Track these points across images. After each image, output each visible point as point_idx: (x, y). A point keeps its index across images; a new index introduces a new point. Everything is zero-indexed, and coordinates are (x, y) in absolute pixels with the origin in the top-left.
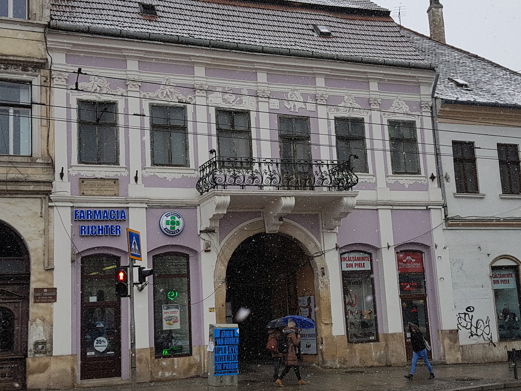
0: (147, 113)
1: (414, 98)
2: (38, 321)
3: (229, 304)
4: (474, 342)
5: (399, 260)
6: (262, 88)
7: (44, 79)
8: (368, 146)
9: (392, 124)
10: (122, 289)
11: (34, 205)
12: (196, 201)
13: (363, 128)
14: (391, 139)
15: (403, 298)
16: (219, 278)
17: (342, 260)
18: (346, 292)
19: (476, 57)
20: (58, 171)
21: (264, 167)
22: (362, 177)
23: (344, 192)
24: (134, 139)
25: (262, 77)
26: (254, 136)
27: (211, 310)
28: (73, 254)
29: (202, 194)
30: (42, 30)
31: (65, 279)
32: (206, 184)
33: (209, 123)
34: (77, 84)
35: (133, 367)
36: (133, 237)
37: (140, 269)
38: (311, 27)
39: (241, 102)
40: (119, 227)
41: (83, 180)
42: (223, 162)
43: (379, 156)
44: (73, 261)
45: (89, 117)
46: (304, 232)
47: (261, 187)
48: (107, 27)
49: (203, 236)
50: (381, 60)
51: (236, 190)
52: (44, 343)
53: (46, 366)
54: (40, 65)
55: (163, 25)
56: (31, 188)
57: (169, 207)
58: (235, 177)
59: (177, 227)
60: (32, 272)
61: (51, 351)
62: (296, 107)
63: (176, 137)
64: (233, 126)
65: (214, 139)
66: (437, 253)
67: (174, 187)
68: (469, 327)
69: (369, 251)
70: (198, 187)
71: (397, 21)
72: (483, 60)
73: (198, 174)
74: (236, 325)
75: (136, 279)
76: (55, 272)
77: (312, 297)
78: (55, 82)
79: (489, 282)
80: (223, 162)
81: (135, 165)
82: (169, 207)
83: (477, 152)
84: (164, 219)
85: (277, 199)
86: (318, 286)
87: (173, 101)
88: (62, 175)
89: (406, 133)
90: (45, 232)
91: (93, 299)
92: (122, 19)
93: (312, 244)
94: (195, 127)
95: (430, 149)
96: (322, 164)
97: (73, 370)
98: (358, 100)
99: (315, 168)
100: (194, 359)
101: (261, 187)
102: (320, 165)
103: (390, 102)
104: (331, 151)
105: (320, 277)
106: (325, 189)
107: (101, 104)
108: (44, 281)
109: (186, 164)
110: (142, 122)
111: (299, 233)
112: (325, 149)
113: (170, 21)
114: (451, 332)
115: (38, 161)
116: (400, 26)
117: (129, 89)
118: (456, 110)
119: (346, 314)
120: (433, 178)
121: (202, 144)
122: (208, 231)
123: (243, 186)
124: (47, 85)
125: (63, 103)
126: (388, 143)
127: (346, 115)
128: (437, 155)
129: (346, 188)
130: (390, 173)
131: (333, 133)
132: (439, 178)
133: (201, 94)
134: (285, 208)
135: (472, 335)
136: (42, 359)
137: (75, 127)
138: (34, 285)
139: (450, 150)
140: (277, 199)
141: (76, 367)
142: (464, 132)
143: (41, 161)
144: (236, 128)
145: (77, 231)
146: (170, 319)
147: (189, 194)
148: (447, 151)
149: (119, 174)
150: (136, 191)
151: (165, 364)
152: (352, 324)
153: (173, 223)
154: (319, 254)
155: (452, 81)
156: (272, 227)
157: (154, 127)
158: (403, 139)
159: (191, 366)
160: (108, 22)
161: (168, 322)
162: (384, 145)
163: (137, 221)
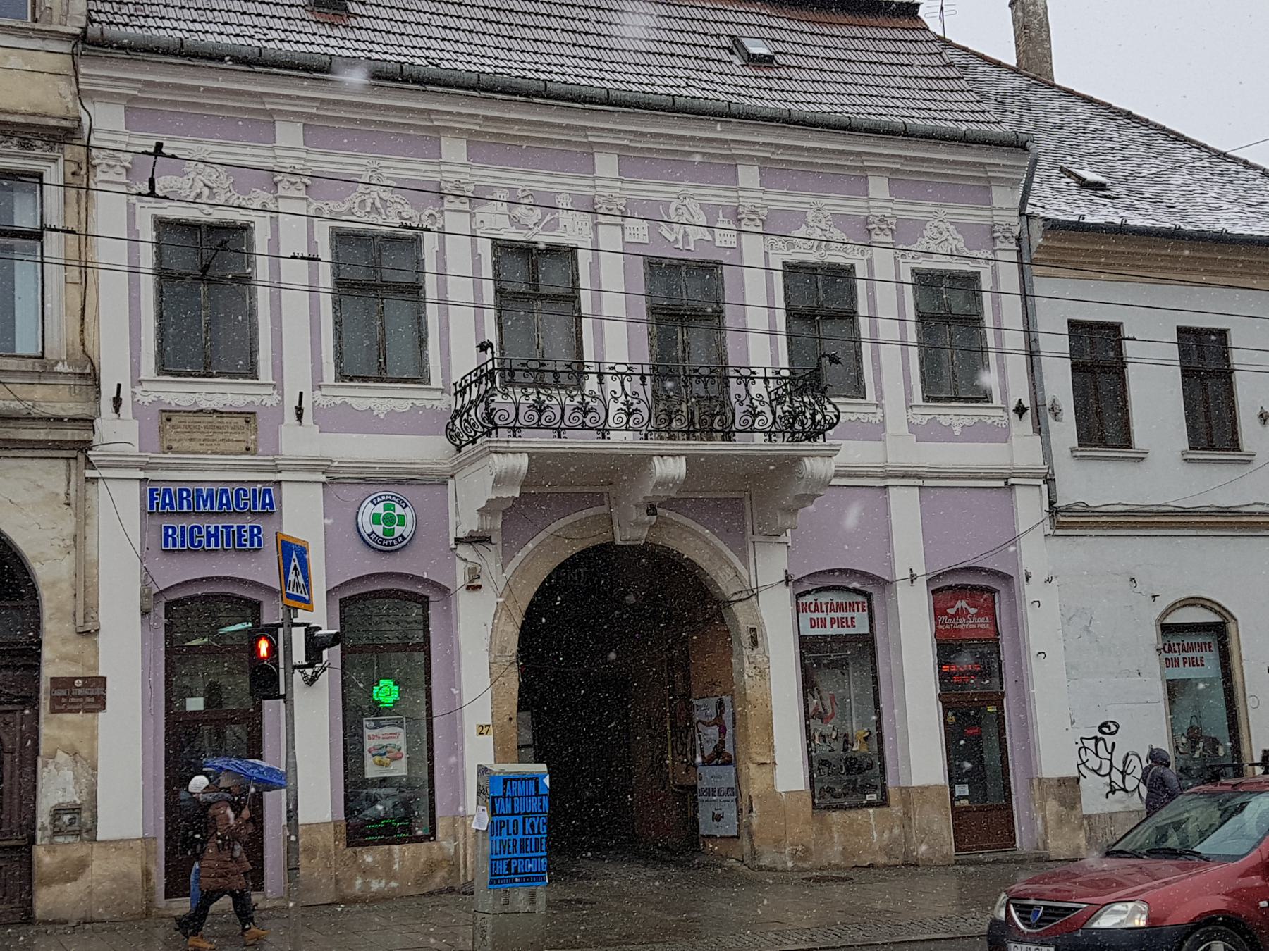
0: (325, 252)
1: (976, 215)
2: (62, 757)
3: (526, 716)
4: (1118, 807)
5: (939, 611)
6: (607, 192)
7: (74, 167)
8: (865, 333)
9: (926, 281)
10: (266, 681)
11: (50, 476)
12: (444, 467)
13: (853, 288)
14: (922, 318)
15: (946, 700)
16: (502, 651)
17: (799, 609)
18: (808, 685)
19: (1129, 115)
20: (108, 392)
21: (612, 384)
22: (849, 409)
23: (805, 446)
24: (294, 316)
25: (606, 164)
26: (586, 308)
27: (482, 729)
28: (144, 596)
29: (459, 449)
30: (66, 48)
31: (125, 655)
32: (469, 426)
33: (477, 278)
34: (152, 182)
35: (292, 869)
36: (293, 554)
37: (310, 631)
38: (726, 42)
39: (554, 224)
40: (259, 528)
41: (168, 415)
42: (512, 372)
43: (890, 357)
44: (145, 613)
45: (182, 261)
46: (707, 542)
47: (604, 432)
48: (225, 40)
49: (463, 551)
50: (843, 118)
51: (543, 441)
52: (75, 810)
53: (82, 865)
54: (62, 135)
55: (364, 35)
56: (41, 434)
57: (376, 481)
58: (540, 408)
59: (398, 531)
60: (45, 638)
61: (93, 830)
62: (687, 240)
63: (397, 310)
64: (534, 282)
65: (490, 316)
66: (1030, 592)
67: (392, 432)
68: (1105, 770)
69: (866, 589)
70: (450, 433)
71: (935, 27)
72: (1146, 123)
73: (450, 402)
74: (543, 767)
75: (299, 656)
76: (101, 638)
77: (726, 699)
78: (100, 176)
79: (1154, 663)
80: (512, 372)
81: (297, 378)
82: (376, 481)
83: (1130, 349)
84: (368, 511)
85: (641, 462)
86: (741, 673)
87: (387, 223)
88: (117, 401)
89: (957, 302)
90: (78, 541)
91: (195, 704)
92: (261, 22)
93: (728, 570)
94: (442, 288)
95: (1015, 341)
96: (752, 378)
97: (147, 875)
98: (839, 220)
99: (735, 388)
100: (441, 848)
101: (604, 432)
102: (747, 379)
103: (799, 217)
104: (774, 345)
105: (747, 652)
106: (759, 438)
107: (211, 228)
108: (74, 660)
109: (421, 377)
110: (314, 275)
111: (697, 543)
112: (759, 341)
113: (380, 25)
114: (1062, 781)
115: (59, 368)
116: (942, 40)
117: (281, 192)
118: (1075, 246)
119: (809, 737)
120: (1020, 410)
121: (460, 329)
122: (477, 540)
123: (559, 432)
124: (80, 185)
125: (120, 228)
126: (912, 328)
127: (811, 258)
128: (1032, 354)
129: (812, 436)
130: (918, 397)
131: (780, 302)
132: (1035, 412)
133: (457, 205)
134: (662, 483)
135: (1113, 791)
136: (73, 848)
137: (148, 285)
138: (49, 671)
139: (1063, 345)
140: (641, 462)
141: (153, 869)
142: (1098, 299)
143: (66, 369)
144: (543, 290)
145: (155, 538)
146: (382, 751)
147: (429, 450)
148: (1056, 345)
149: (257, 400)
150: (297, 441)
151: (369, 859)
152: (824, 763)
153: (389, 520)
154: (744, 596)
155: (1071, 174)
156: (630, 530)
157: (342, 286)
158: (949, 318)
159: (433, 866)
160: (229, 29)
161: (378, 758)
162: (903, 331)
163: (302, 515)
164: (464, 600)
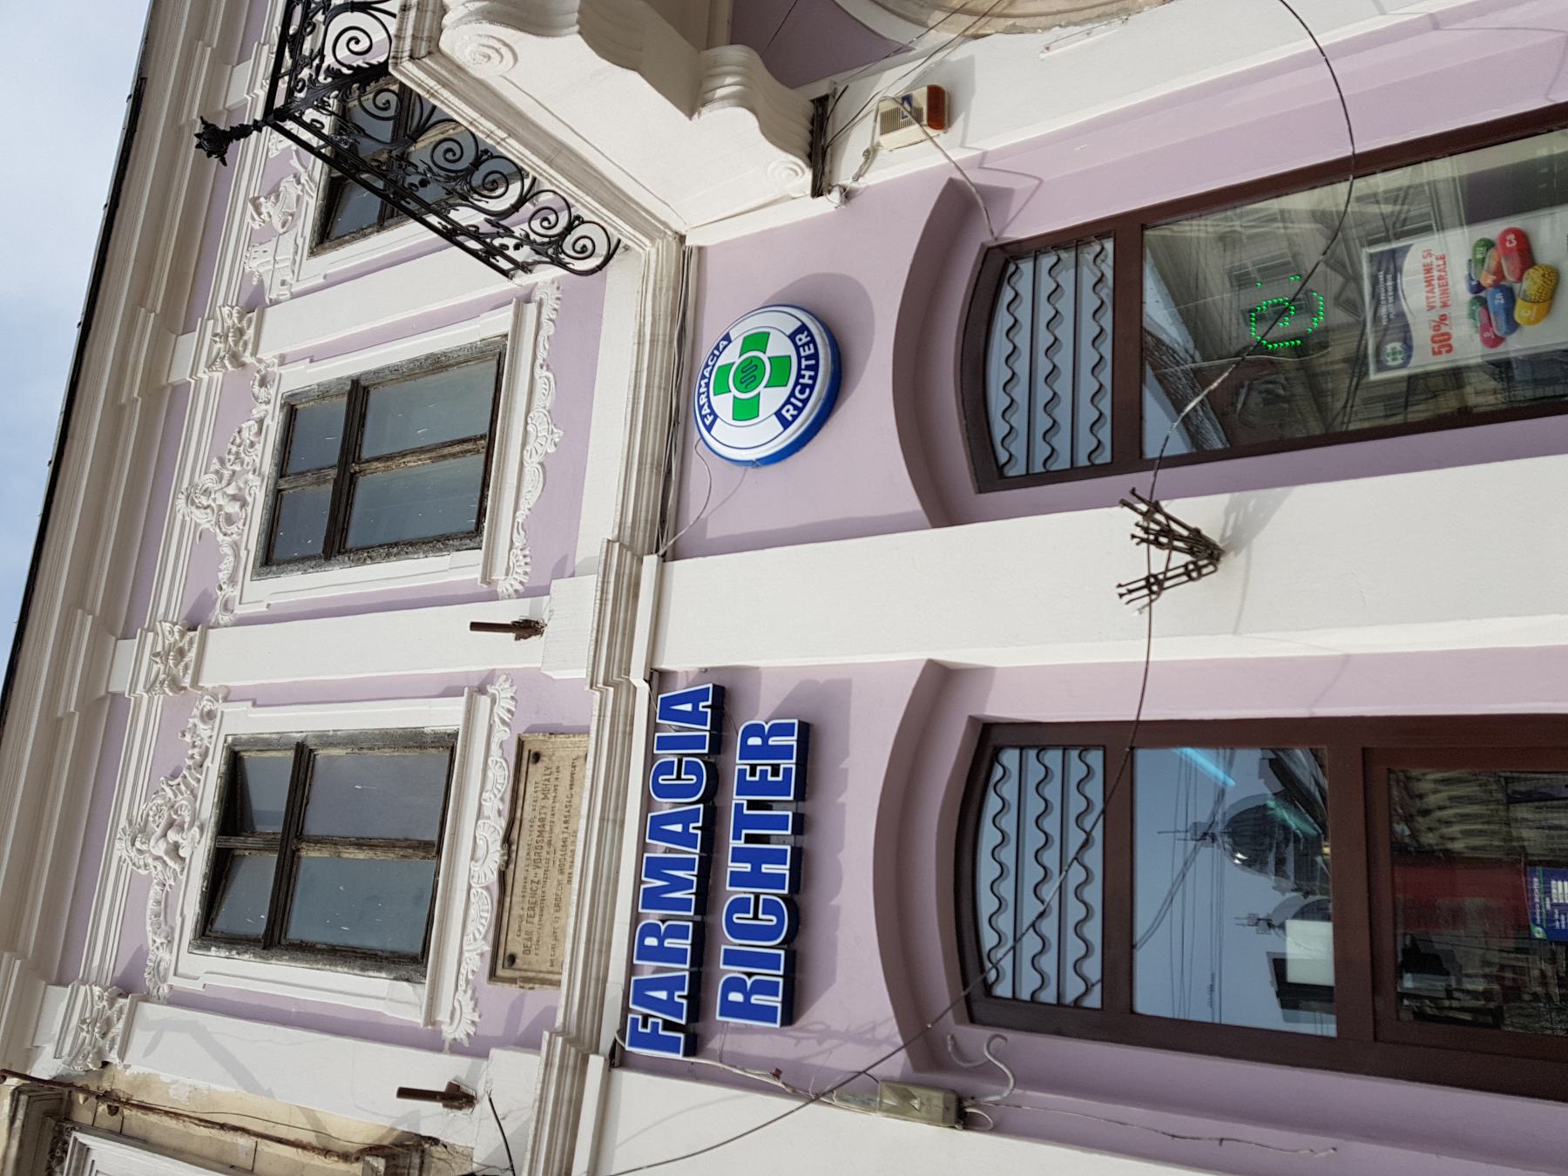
44: (962, 1116)
49: (846, 167)
59: (780, 346)
81: (439, 644)
146: (1499, 299)
161: (1522, 312)
164: (986, 137)
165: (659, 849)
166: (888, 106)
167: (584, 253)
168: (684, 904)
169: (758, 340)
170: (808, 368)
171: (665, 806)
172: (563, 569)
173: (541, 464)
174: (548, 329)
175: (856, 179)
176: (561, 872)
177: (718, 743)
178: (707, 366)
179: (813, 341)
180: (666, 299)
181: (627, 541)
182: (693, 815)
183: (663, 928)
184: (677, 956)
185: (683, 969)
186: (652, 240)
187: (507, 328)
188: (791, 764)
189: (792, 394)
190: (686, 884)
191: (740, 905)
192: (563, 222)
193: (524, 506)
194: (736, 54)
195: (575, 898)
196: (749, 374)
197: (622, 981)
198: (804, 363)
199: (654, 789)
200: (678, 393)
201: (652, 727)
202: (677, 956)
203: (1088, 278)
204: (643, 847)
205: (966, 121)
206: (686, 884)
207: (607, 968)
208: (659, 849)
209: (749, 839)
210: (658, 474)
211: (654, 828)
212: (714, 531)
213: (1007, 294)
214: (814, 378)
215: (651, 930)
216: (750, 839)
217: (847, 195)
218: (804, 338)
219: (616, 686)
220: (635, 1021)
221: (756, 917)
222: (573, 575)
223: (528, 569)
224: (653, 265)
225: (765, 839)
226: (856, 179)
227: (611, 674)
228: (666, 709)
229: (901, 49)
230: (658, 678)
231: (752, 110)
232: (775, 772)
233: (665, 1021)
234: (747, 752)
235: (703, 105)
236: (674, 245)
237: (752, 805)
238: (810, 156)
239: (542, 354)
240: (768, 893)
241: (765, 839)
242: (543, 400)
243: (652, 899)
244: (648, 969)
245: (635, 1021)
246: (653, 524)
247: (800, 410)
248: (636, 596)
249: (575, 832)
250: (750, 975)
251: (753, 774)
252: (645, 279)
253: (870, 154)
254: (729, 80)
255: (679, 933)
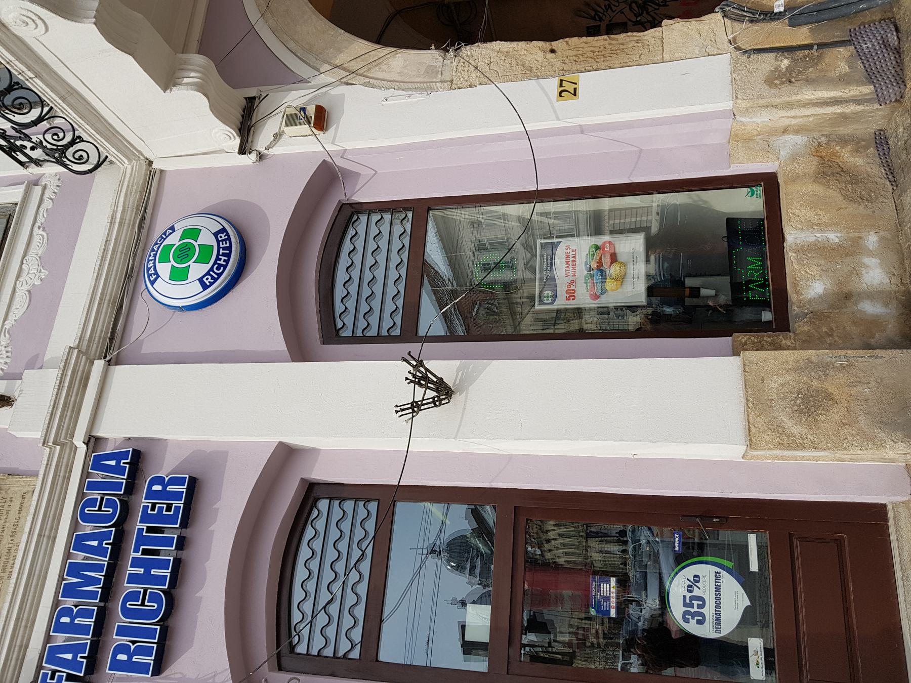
27: (567, 91)
49: (262, 140)
59: (206, 238)
100: (794, 158)
164: (347, 140)
165: (79, 557)
166: (291, 111)
167: (80, 160)
168: (93, 595)
169: (193, 233)
170: (223, 255)
171: (88, 528)
172: (34, 363)
173: (29, 291)
174: (47, 204)
175: (267, 148)
176: (4, 571)
177: (131, 488)
178: (156, 243)
179: (229, 239)
180: (134, 199)
181: (84, 348)
182: (106, 535)
183: (75, 610)
184: (83, 629)
185: (87, 639)
186: (130, 160)
187: (18, 199)
188: (180, 504)
189: (211, 269)
190: (95, 581)
191: (133, 596)
192: (69, 138)
193: (12, 318)
194: (200, 59)
195: (11, 589)
196: (184, 253)
197: (40, 647)
198: (221, 251)
199: (82, 514)
200: (134, 257)
201: (85, 474)
202: (83, 629)
203: (398, 229)
204: (67, 555)
205: (337, 129)
206: (95, 581)
207: (29, 638)
208: (79, 557)
209: (145, 552)
210: (113, 308)
211: (78, 542)
212: (146, 349)
213: (351, 232)
214: (227, 262)
215: (67, 612)
216: (145, 552)
217: (261, 157)
218: (223, 236)
219: (63, 445)
220: (45, 675)
221: (143, 604)
222: (41, 368)
223: (8, 361)
224: (128, 176)
225: (156, 552)
226: (267, 148)
227: (58, 435)
228: (98, 464)
229: (302, 81)
230: (93, 441)
231: (205, 95)
232: (169, 508)
233: (68, 674)
234: (151, 494)
235: (174, 86)
236: (144, 166)
237: (149, 530)
238: (240, 130)
239: (41, 220)
240: (153, 588)
241: (156, 552)
242: (37, 248)
243: (69, 591)
244: (60, 639)
245: (45, 675)
246: (104, 340)
247: (215, 280)
248: (85, 386)
249: (18, 543)
250: (134, 642)
251: (153, 509)
252: (121, 183)
253: (277, 136)
254: (193, 74)
255: (86, 614)
